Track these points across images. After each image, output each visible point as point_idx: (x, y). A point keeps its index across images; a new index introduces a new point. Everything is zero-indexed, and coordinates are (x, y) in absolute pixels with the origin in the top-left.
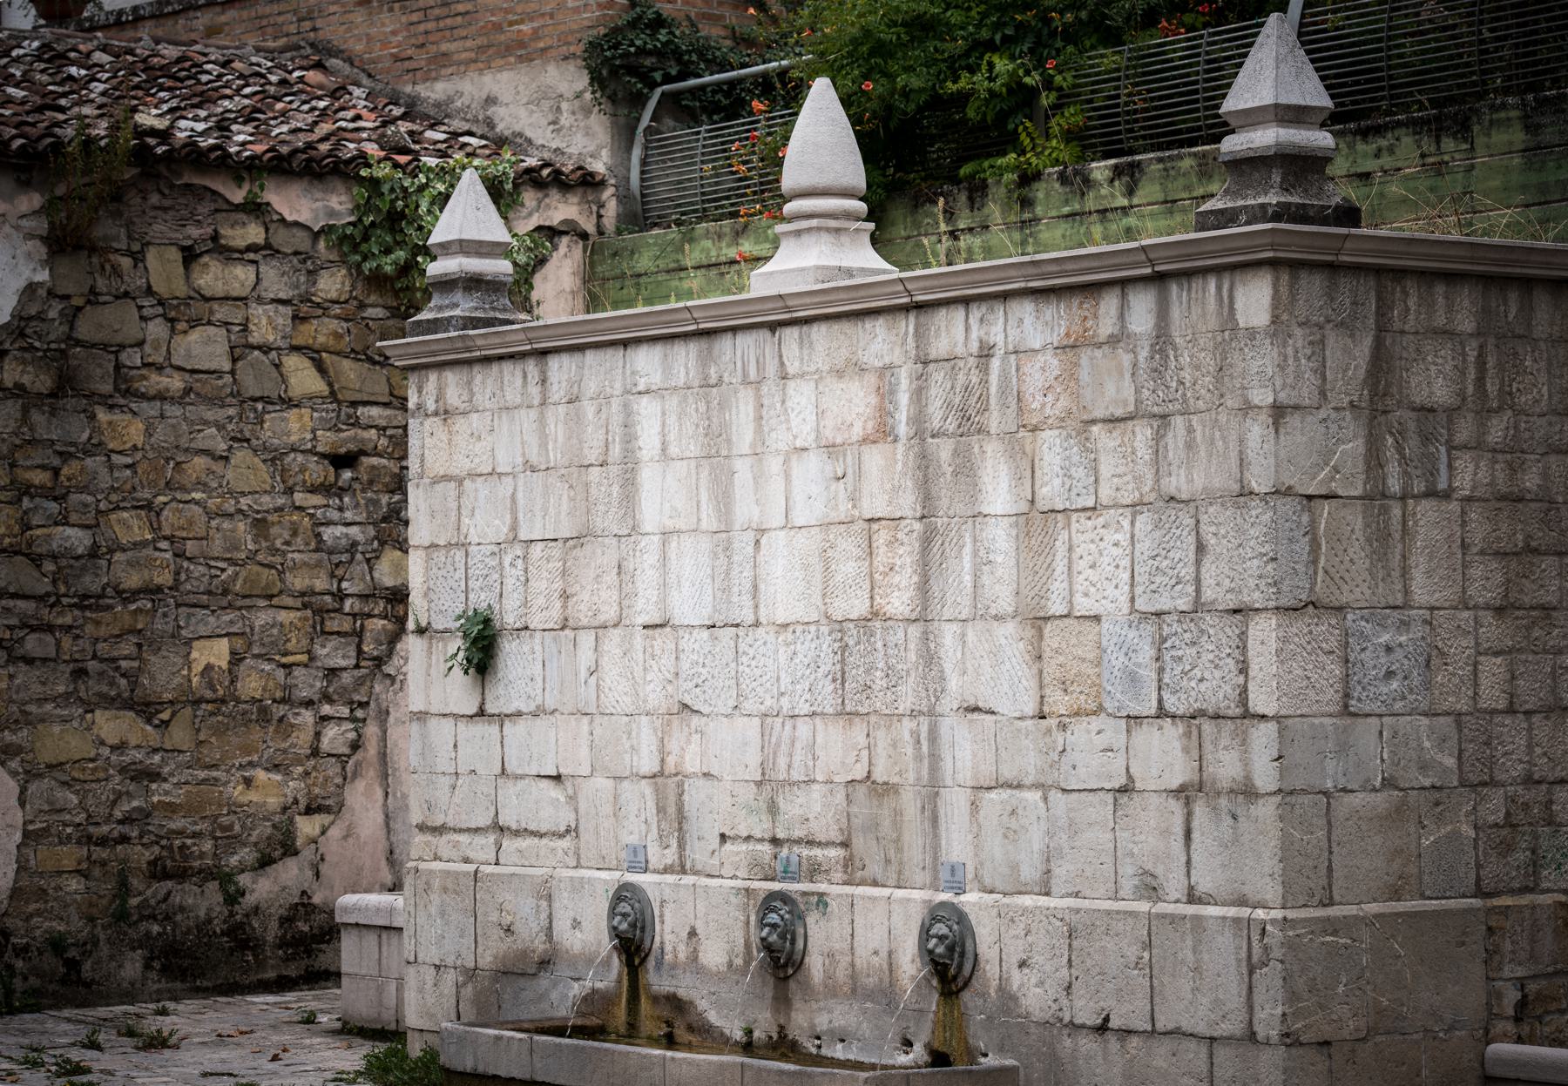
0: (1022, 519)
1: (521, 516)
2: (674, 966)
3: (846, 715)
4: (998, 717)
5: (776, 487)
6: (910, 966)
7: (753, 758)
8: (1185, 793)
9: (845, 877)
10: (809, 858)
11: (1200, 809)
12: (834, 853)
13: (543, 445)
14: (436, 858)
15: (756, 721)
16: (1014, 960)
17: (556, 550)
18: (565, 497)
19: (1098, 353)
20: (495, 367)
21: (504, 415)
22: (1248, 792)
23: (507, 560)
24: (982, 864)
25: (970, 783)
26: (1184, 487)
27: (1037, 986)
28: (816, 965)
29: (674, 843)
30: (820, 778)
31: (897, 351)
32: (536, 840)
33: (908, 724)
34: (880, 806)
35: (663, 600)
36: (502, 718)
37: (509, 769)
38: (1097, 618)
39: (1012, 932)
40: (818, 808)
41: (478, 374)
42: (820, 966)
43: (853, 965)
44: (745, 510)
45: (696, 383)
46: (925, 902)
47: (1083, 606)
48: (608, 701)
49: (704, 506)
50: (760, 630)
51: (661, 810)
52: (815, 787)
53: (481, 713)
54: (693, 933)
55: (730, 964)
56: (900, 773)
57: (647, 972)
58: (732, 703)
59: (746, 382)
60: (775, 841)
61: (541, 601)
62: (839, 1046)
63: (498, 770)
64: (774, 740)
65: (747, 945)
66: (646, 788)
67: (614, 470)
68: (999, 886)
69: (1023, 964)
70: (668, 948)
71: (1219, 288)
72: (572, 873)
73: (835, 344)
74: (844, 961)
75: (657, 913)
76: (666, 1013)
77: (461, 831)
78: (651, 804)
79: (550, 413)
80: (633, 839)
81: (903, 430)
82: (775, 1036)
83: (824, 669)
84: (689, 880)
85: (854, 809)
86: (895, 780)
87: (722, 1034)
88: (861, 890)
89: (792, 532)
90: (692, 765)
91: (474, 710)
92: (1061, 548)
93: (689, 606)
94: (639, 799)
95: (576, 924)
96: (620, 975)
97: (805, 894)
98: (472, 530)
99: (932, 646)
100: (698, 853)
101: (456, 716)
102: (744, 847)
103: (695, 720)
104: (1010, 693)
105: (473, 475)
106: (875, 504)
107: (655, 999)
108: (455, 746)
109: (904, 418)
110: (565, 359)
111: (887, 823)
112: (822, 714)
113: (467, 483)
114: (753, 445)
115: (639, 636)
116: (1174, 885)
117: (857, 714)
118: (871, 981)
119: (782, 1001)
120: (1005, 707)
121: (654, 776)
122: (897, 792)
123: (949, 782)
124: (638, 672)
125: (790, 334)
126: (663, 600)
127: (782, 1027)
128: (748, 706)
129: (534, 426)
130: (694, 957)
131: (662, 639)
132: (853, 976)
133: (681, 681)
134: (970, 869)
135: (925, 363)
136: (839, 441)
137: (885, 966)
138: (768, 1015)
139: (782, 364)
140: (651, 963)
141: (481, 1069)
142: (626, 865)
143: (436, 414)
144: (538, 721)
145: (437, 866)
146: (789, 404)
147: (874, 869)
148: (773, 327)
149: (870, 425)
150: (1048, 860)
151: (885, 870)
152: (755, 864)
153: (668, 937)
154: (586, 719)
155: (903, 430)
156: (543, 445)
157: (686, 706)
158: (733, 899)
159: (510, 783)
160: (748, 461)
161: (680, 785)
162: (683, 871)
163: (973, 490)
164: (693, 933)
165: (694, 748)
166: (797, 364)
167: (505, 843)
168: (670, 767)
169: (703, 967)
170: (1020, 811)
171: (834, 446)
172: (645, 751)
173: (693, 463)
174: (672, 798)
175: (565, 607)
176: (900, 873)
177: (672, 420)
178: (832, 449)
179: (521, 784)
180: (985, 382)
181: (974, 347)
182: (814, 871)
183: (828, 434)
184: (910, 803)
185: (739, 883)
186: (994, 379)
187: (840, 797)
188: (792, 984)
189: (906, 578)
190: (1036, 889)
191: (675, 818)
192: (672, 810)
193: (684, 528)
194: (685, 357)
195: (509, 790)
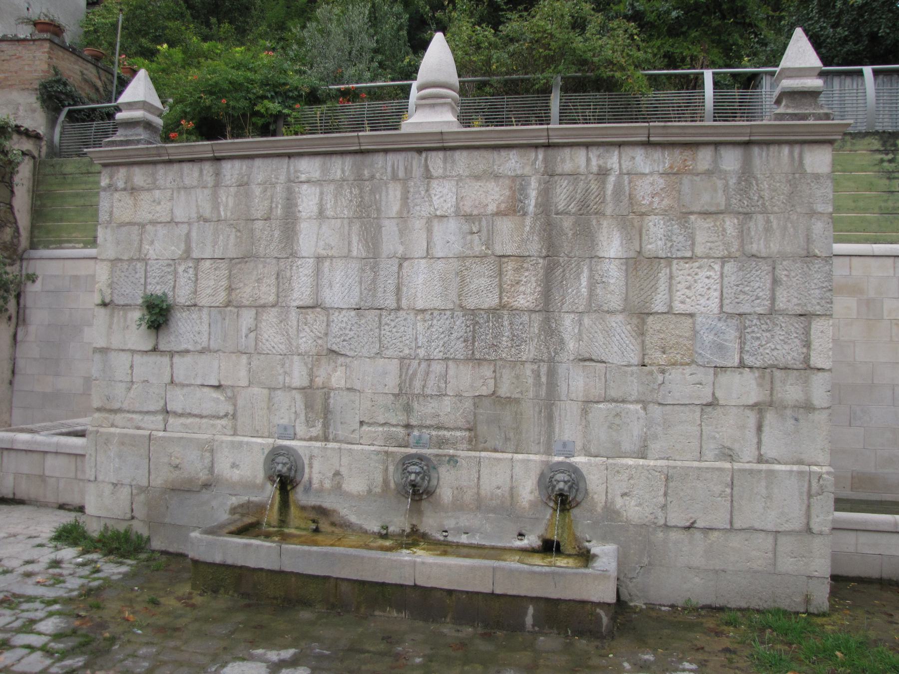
0: (631, 261)
1: (194, 245)
3: (474, 360)
4: (609, 365)
8: (759, 408)
10: (438, 436)
14: (112, 425)
15: (396, 362)
17: (223, 265)
18: (232, 237)
20: (176, 167)
21: (182, 192)
22: (809, 407)
23: (180, 269)
26: (763, 250)
32: (198, 420)
36: (172, 354)
37: (176, 380)
38: (691, 315)
41: (161, 170)
43: (478, 494)
46: (542, 462)
53: (155, 350)
55: (370, 491)
56: (521, 392)
57: (296, 493)
58: (375, 350)
60: (408, 426)
61: (209, 291)
62: (464, 536)
63: (167, 379)
64: (410, 372)
71: (791, 153)
77: (134, 412)
80: (285, 422)
84: (331, 445)
87: (361, 528)
88: (483, 454)
89: (432, 261)
91: (150, 347)
95: (234, 466)
97: (437, 455)
98: (151, 252)
101: (133, 352)
102: (381, 429)
103: (341, 360)
104: (619, 352)
105: (154, 223)
108: (132, 367)
109: (533, 202)
110: (237, 164)
113: (149, 228)
114: (400, 212)
117: (485, 360)
123: (563, 397)
124: (292, 332)
128: (389, 353)
133: (330, 338)
143: (125, 189)
144: (204, 356)
145: (112, 430)
148: (419, 151)
150: (645, 440)
155: (531, 209)
162: (326, 439)
164: (337, 474)
170: (623, 415)
172: (296, 374)
173: (346, 222)
179: (186, 390)
184: (529, 410)
186: (610, 187)
190: (635, 455)
192: (319, 406)
193: (336, 255)
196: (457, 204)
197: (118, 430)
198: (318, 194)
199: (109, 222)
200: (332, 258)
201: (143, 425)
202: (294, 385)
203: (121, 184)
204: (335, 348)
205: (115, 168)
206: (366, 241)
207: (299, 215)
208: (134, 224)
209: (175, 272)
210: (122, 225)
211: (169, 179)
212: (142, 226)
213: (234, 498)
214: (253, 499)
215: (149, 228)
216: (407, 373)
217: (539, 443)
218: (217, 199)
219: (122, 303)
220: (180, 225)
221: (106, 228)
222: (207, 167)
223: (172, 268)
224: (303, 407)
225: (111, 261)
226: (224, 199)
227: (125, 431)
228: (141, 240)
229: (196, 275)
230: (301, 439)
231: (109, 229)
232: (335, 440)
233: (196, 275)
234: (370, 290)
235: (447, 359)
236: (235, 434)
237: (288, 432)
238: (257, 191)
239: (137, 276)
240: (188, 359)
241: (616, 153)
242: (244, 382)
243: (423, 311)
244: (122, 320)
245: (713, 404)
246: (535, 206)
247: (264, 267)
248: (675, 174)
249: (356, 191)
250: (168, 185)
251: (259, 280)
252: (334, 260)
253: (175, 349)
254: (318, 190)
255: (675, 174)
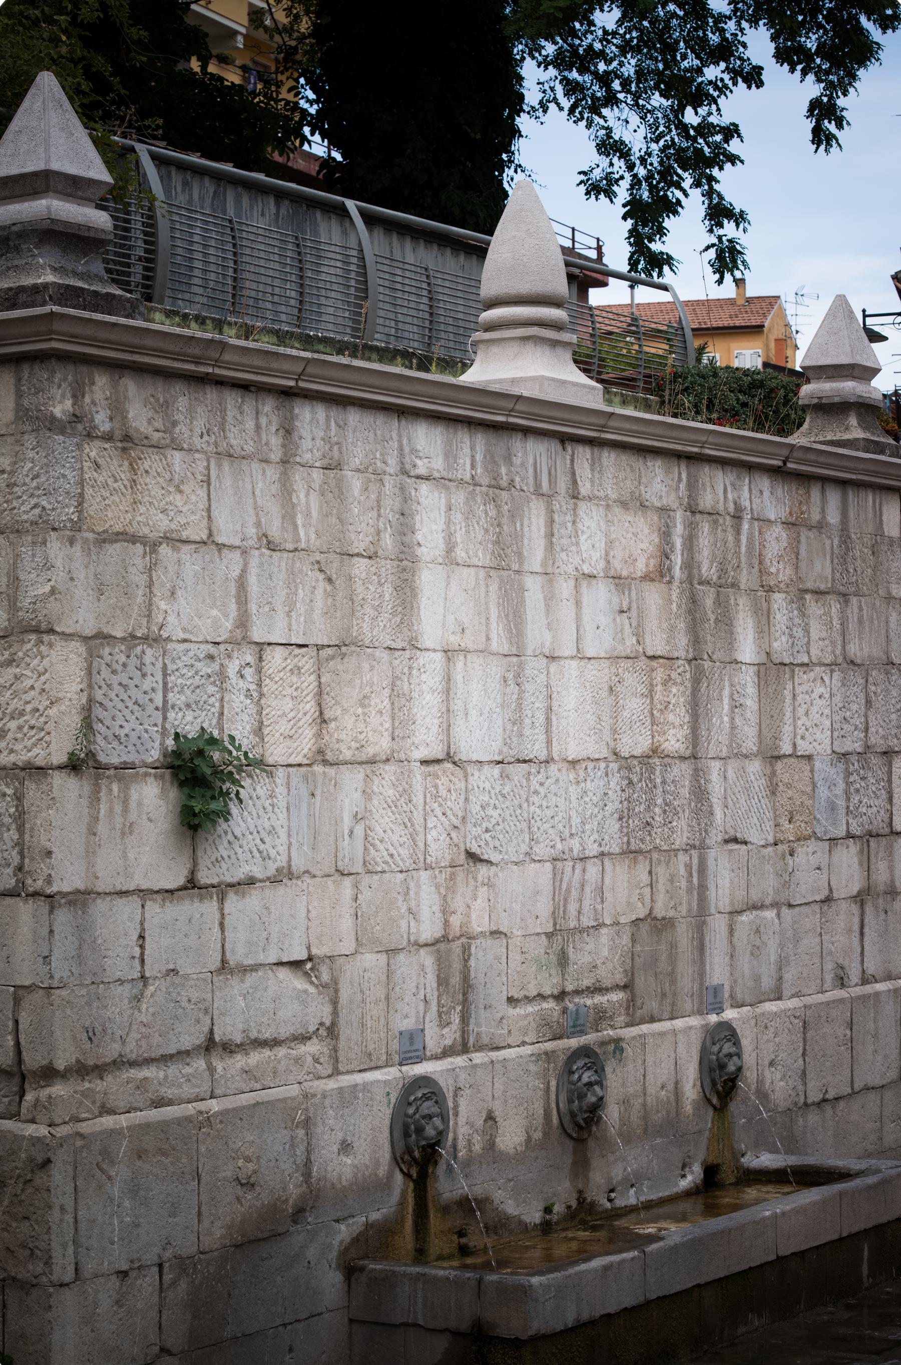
0: (762, 669)
1: (253, 608)
2: (468, 1163)
3: (630, 853)
4: (750, 847)
5: (566, 612)
6: (691, 1091)
7: (544, 907)
8: (860, 899)
9: (628, 1019)
11: (869, 909)
12: (617, 996)
13: (289, 516)
14: (106, 1110)
15: (548, 866)
16: (767, 1062)
17: (306, 660)
18: (319, 592)
19: (811, 534)
20: (211, 395)
23: (232, 668)
24: (735, 981)
25: (728, 909)
26: (858, 654)
27: (781, 1080)
28: (612, 1114)
29: (456, 1019)
30: (608, 922)
31: (673, 496)
32: (267, 1053)
33: (682, 858)
34: (658, 942)
35: (447, 728)
36: (222, 890)
38: (809, 758)
39: (765, 1037)
40: (605, 952)
41: (182, 399)
42: (616, 1115)
43: (644, 1105)
44: (537, 635)
45: (485, 481)
46: (703, 1026)
47: (804, 747)
48: (379, 856)
49: (494, 625)
50: (553, 768)
51: (442, 981)
52: (604, 931)
53: (191, 884)
54: (490, 1117)
55: (529, 1140)
56: (675, 908)
57: (436, 1179)
58: (524, 848)
59: (538, 492)
61: (284, 727)
62: (632, 1191)
63: (214, 962)
64: (564, 886)
65: (547, 1115)
66: (427, 959)
67: (387, 567)
68: (748, 1001)
69: (771, 1064)
70: (461, 1144)
72: (331, 1085)
73: (622, 475)
74: (637, 1103)
75: (451, 1105)
76: (456, 1221)
77: (148, 1061)
78: (431, 979)
79: (298, 477)
80: (408, 1024)
81: (677, 572)
82: (574, 1204)
83: (610, 808)
84: (479, 1058)
85: (638, 948)
86: (671, 914)
87: (520, 1222)
88: (645, 1028)
89: (583, 663)
90: (479, 923)
91: (181, 881)
92: (788, 693)
93: (478, 738)
94: (418, 975)
95: (346, 1147)
96: (403, 1195)
97: (603, 1044)
98: (172, 619)
99: (702, 782)
100: (484, 1026)
101: (144, 894)
102: (530, 1009)
103: (483, 871)
104: (758, 824)
105: (176, 541)
106: (656, 644)
107: (446, 1210)
108: (142, 937)
110: (321, 412)
111: (663, 957)
112: (610, 854)
113: (164, 550)
114: (544, 564)
115: (418, 771)
116: (854, 975)
117: (639, 852)
118: (657, 1118)
119: (581, 1165)
120: (756, 838)
121: (437, 942)
122: (673, 926)
123: (713, 911)
125: (584, 453)
126: (447, 728)
127: (580, 1192)
128: (541, 851)
129: (275, 488)
130: (491, 1146)
131: (446, 774)
132: (645, 1117)
133: (469, 826)
134: (727, 988)
135: (693, 513)
136: (625, 573)
137: (672, 1097)
138: (567, 1184)
139: (575, 482)
140: (442, 1168)
141: (585, 1316)
142: (396, 1058)
143: (108, 437)
144: (281, 890)
145: (108, 1121)
146: (580, 526)
147: (653, 1005)
148: (564, 439)
149: (652, 562)
150: (780, 969)
151: (661, 1004)
152: (544, 1022)
153: (463, 1130)
154: (347, 882)
155: (677, 572)
156: (289, 516)
157: (471, 856)
158: (533, 1068)
159: (234, 981)
160: (539, 579)
161: (466, 949)
162: (465, 1049)
163: (730, 641)
164: (490, 1117)
165: (480, 904)
166: (588, 485)
167: (219, 1066)
168: (455, 929)
169: (501, 1152)
170: (762, 929)
171: (620, 578)
172: (425, 913)
174: (457, 966)
175: (319, 735)
176: (673, 1004)
177: (458, 517)
178: (619, 581)
179: (251, 979)
180: (738, 541)
181: (731, 508)
182: (601, 1017)
183: (617, 565)
184: (683, 934)
185: (528, 1050)
187: (626, 939)
188: (591, 1143)
189: (678, 716)
191: (458, 988)
192: (456, 980)
193: (471, 646)
194: (470, 450)
195: (236, 989)
196: (607, 554)
197: (124, 1121)
198: (443, 508)
199: (77, 527)
200: (466, 651)
201: (169, 1093)
202: (422, 940)
203: (102, 421)
204: (475, 849)
205: (84, 369)
206: (507, 616)
207: (419, 551)
208: (133, 539)
209: (222, 675)
210: (106, 539)
211: (199, 424)
212: (153, 546)
213: (343, 1227)
214: (375, 1216)
215: (164, 550)
216: (560, 889)
217: (692, 995)
218: (290, 494)
219: (115, 761)
220: (225, 551)
221: (72, 541)
222: (267, 408)
223: (216, 666)
224: (435, 985)
225: (86, 639)
226: (302, 496)
227: (137, 1117)
228: (150, 585)
229: (259, 685)
230: (435, 1057)
231: (77, 547)
232: (480, 1048)
233: (259, 685)
234: (514, 724)
235: (603, 854)
236: (336, 1072)
237: (411, 1049)
238: (355, 484)
239: (147, 684)
240: (254, 900)
241: (747, 481)
242: (348, 946)
243: (574, 763)
244: (118, 809)
245: (828, 900)
246: (681, 568)
247: (372, 668)
248: (793, 524)
249: (492, 513)
250: (198, 443)
251: (364, 701)
252: (469, 656)
253: (229, 879)
254: (443, 500)
255: (793, 524)
